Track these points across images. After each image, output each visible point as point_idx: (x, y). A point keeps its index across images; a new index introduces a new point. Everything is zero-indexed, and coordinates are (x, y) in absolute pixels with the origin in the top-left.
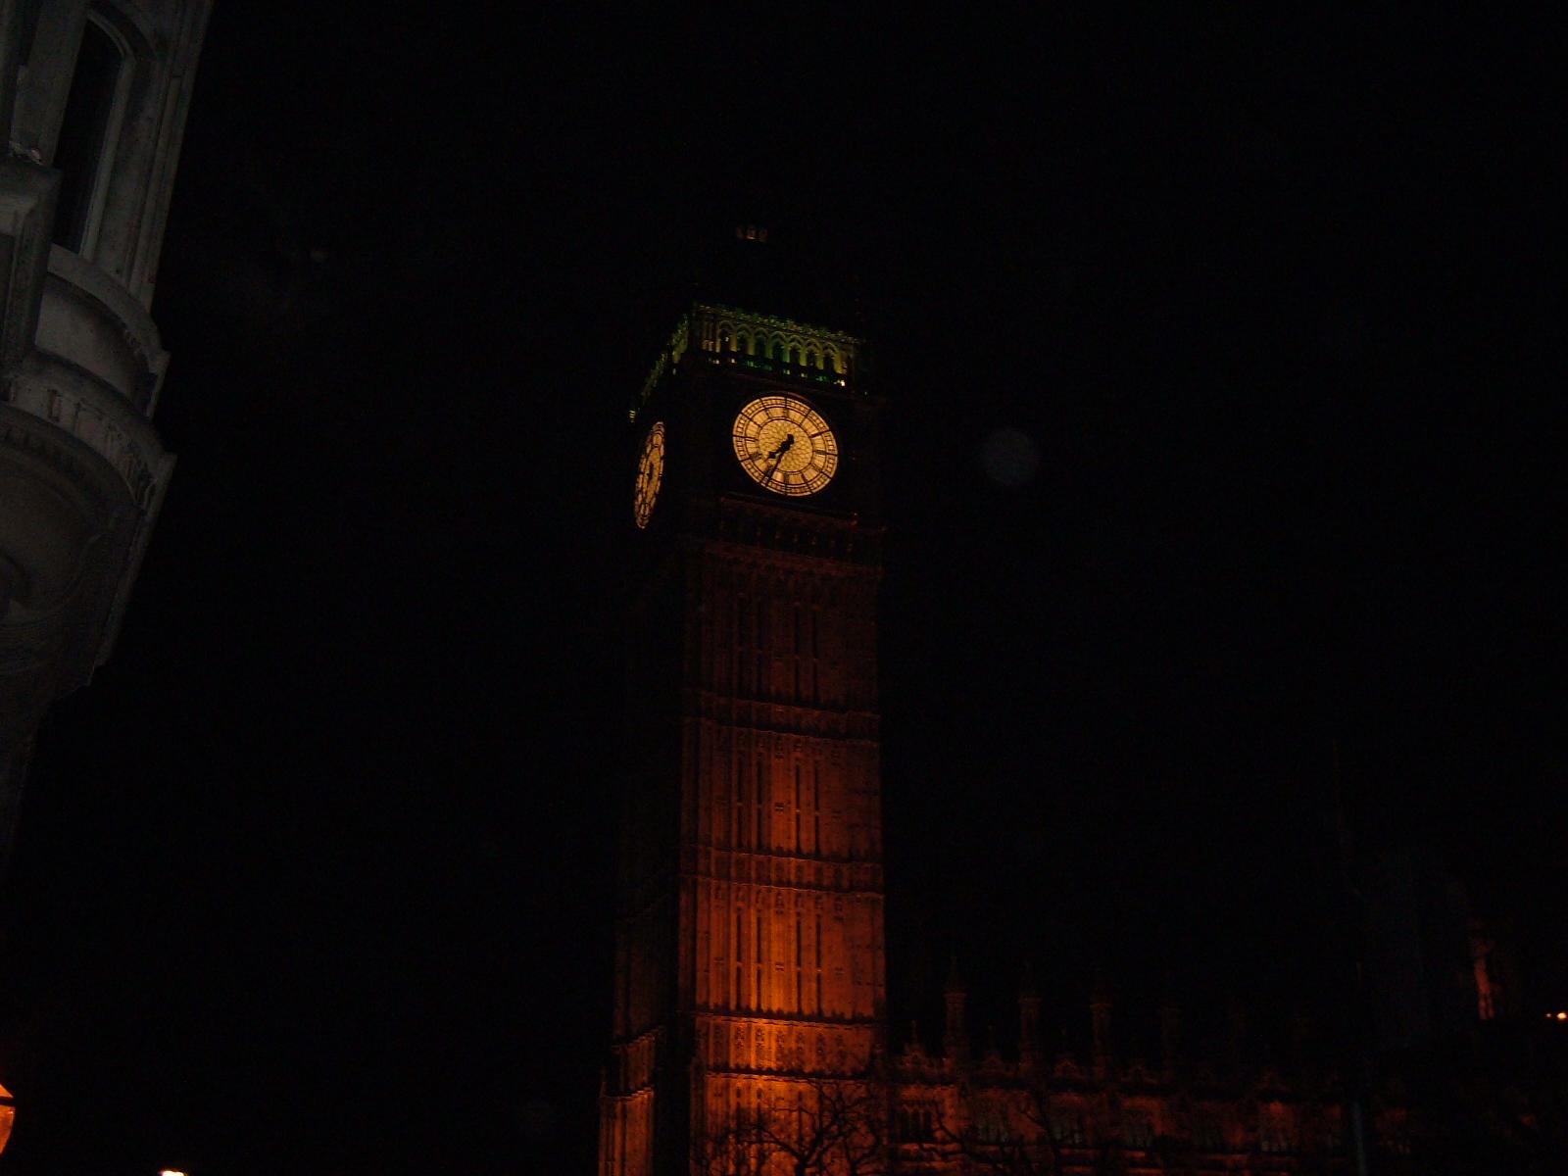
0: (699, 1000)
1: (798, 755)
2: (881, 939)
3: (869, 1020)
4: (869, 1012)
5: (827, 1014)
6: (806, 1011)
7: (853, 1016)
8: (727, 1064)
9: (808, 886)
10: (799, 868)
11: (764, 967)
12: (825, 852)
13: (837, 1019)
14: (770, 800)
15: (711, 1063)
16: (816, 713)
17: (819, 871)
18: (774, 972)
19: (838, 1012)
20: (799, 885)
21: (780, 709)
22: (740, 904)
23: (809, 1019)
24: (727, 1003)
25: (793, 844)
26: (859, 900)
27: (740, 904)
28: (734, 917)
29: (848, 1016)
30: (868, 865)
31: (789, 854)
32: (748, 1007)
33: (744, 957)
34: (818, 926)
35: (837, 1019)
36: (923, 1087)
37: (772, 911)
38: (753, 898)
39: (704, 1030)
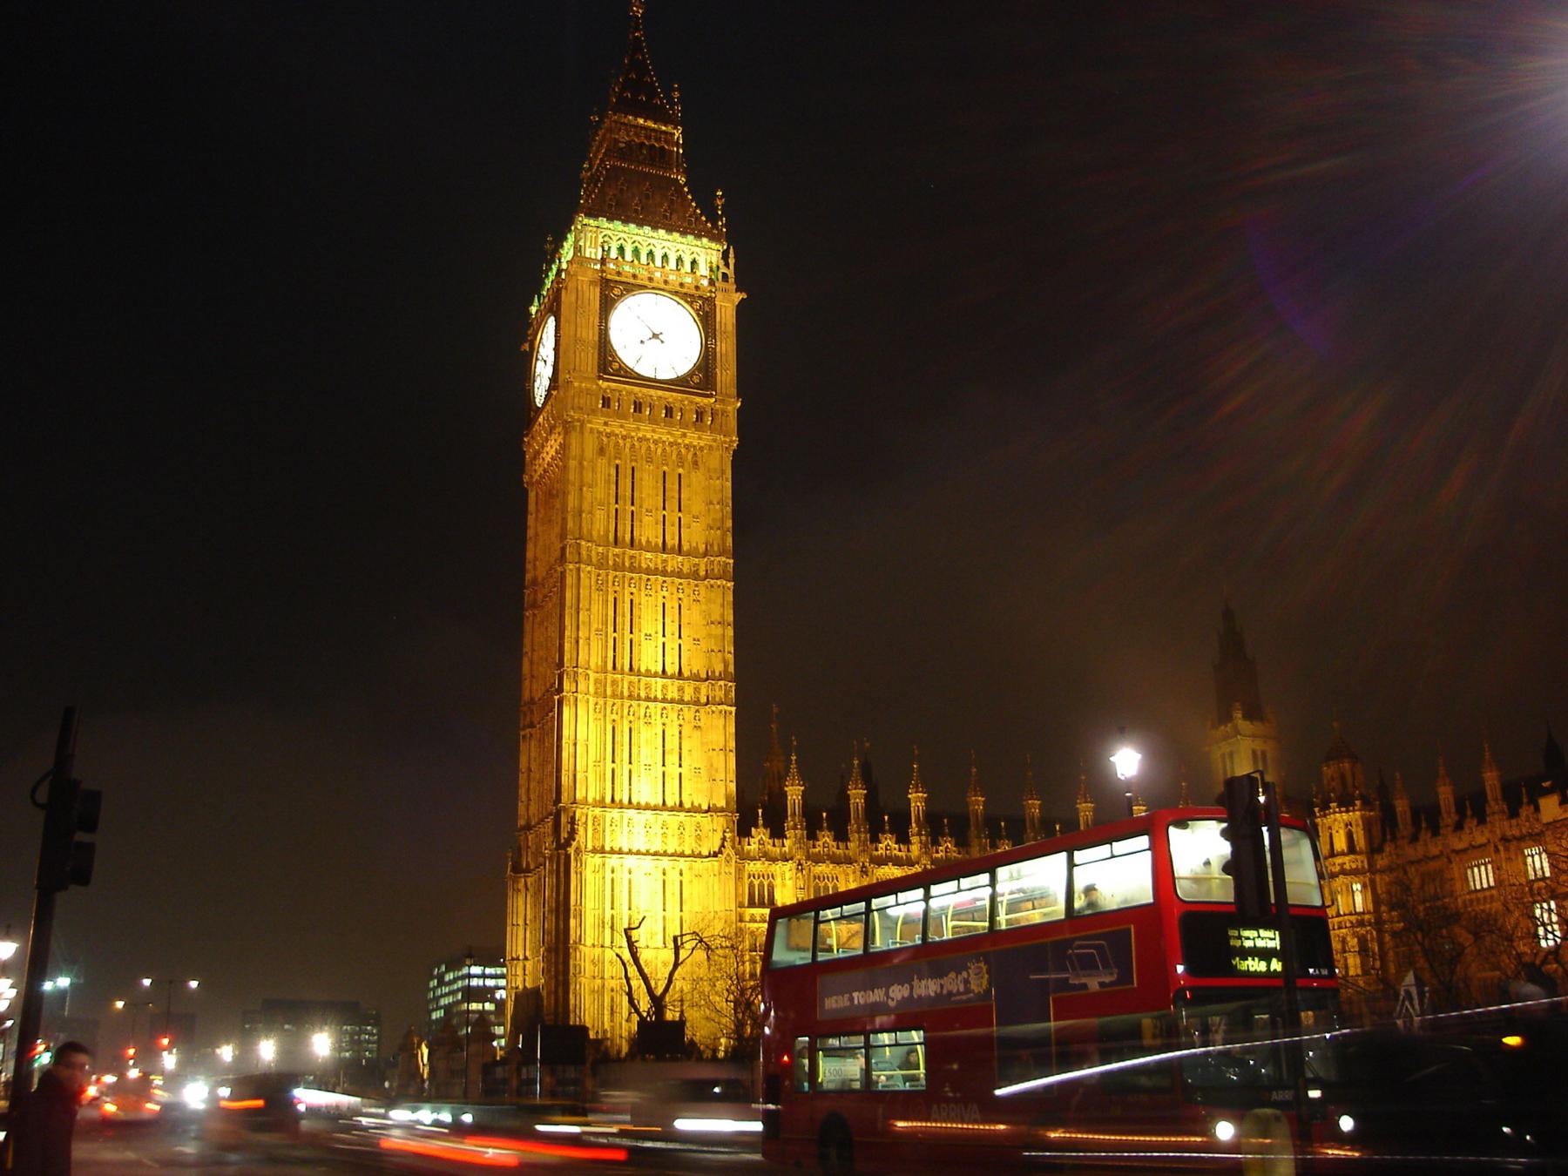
0: (579, 796)
1: (666, 594)
2: (732, 744)
3: (722, 810)
4: (722, 803)
5: (687, 805)
6: (670, 803)
7: (709, 807)
8: (603, 847)
9: (672, 701)
10: (664, 687)
11: (634, 767)
12: (686, 673)
13: (695, 810)
14: (640, 631)
15: (590, 847)
16: (680, 558)
17: (681, 689)
18: (643, 771)
19: (696, 804)
20: (664, 700)
21: (649, 555)
22: (614, 716)
23: (672, 809)
24: (603, 798)
25: (660, 669)
26: (713, 712)
27: (614, 716)
28: (609, 728)
29: (705, 807)
30: (722, 683)
31: (655, 675)
32: (621, 801)
33: (617, 759)
34: (680, 733)
35: (695, 810)
36: (767, 863)
37: (642, 721)
38: (626, 711)
39: (584, 820)
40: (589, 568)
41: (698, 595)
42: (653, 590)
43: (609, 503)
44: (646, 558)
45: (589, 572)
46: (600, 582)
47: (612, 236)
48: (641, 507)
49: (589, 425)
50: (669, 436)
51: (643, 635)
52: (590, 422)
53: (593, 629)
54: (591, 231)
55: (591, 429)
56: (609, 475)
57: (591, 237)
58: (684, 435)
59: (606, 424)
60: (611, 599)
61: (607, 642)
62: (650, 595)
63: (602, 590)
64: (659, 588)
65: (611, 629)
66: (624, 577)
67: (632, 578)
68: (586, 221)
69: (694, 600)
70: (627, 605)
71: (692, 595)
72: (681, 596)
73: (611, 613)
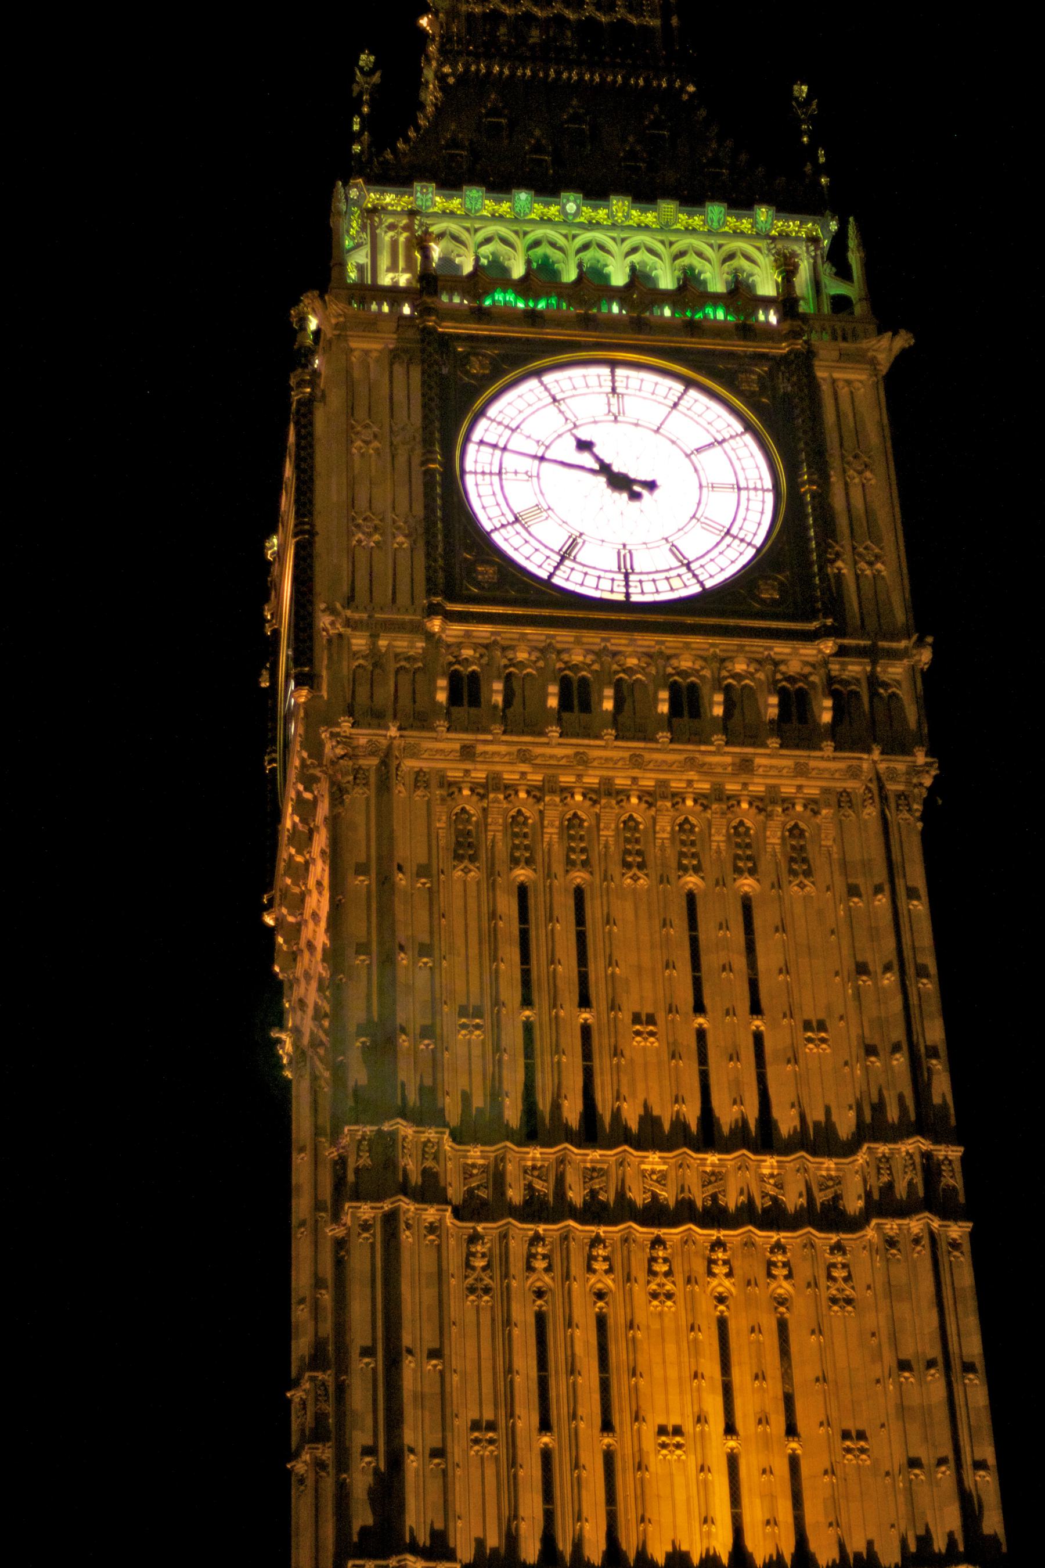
14: (637, 1417)
16: (769, 1164)
40: (431, 1213)
41: (847, 1279)
42: (679, 1278)
43: (497, 1002)
44: (643, 1174)
45: (432, 1229)
46: (480, 1263)
47: (465, 236)
48: (614, 1006)
49: (410, 764)
50: (692, 775)
51: (648, 1430)
52: (413, 752)
53: (461, 1424)
54: (392, 227)
55: (419, 773)
56: (493, 915)
57: (394, 243)
58: (745, 766)
59: (467, 753)
60: (523, 1314)
61: (513, 1463)
62: (669, 1296)
63: (487, 1290)
64: (699, 1267)
65: (527, 1418)
66: (565, 1238)
67: (596, 1241)
68: (372, 197)
69: (834, 1301)
70: (585, 1338)
71: (823, 1281)
72: (784, 1288)
73: (525, 1363)
